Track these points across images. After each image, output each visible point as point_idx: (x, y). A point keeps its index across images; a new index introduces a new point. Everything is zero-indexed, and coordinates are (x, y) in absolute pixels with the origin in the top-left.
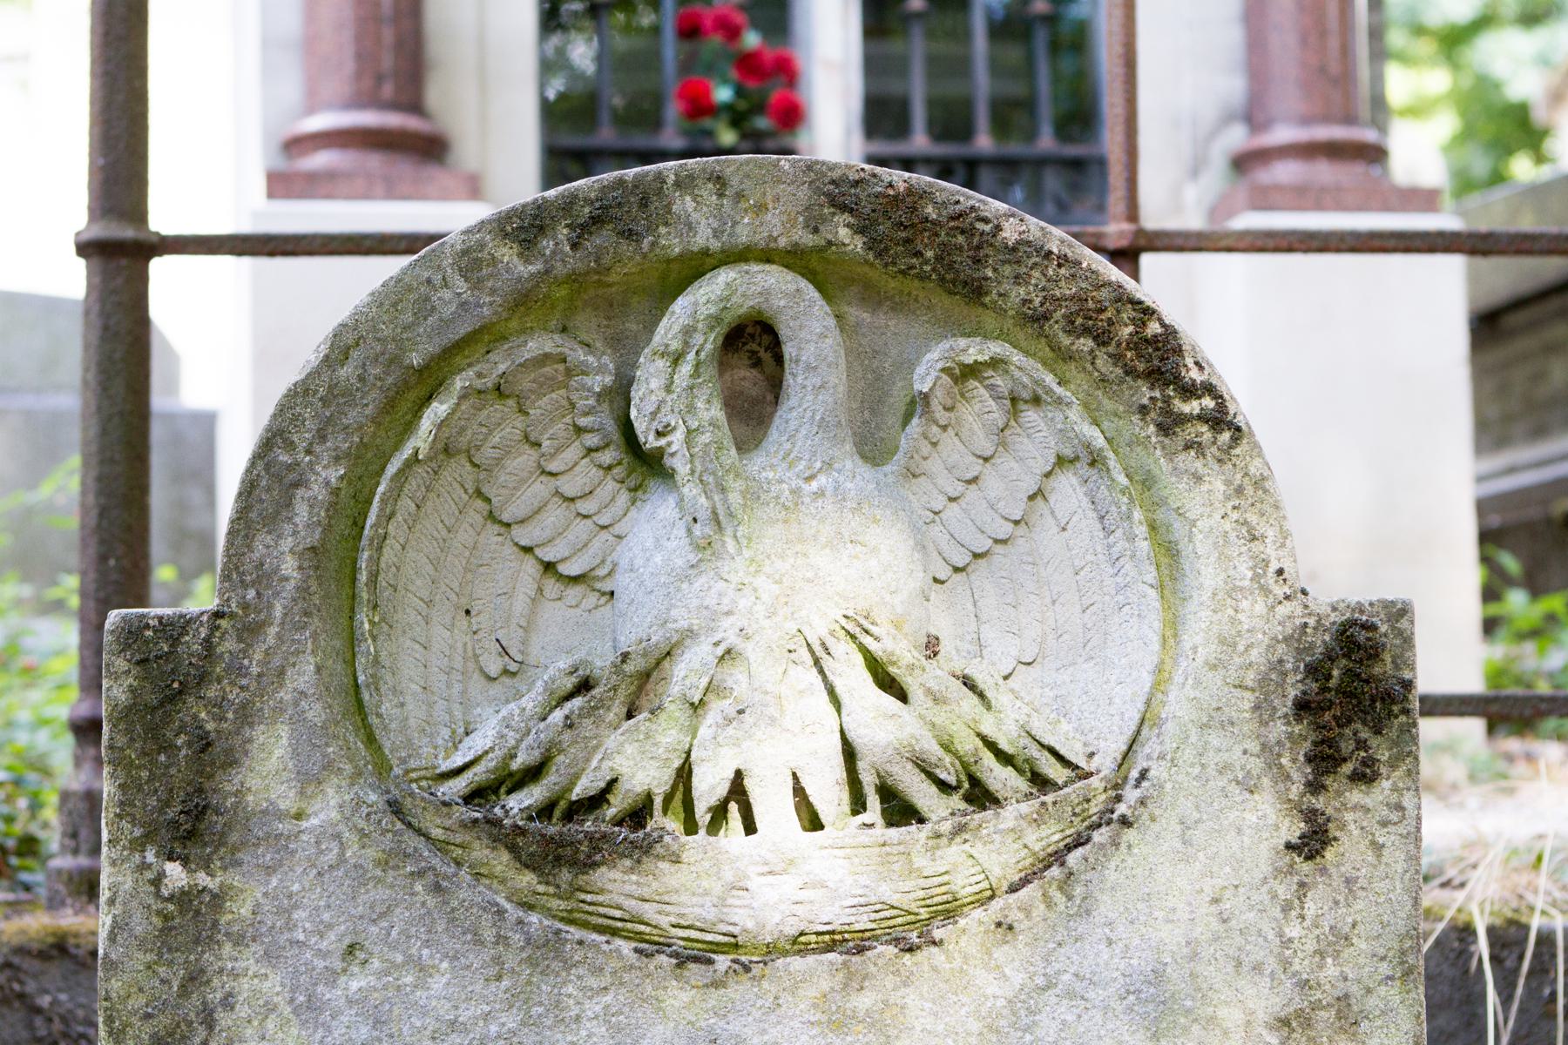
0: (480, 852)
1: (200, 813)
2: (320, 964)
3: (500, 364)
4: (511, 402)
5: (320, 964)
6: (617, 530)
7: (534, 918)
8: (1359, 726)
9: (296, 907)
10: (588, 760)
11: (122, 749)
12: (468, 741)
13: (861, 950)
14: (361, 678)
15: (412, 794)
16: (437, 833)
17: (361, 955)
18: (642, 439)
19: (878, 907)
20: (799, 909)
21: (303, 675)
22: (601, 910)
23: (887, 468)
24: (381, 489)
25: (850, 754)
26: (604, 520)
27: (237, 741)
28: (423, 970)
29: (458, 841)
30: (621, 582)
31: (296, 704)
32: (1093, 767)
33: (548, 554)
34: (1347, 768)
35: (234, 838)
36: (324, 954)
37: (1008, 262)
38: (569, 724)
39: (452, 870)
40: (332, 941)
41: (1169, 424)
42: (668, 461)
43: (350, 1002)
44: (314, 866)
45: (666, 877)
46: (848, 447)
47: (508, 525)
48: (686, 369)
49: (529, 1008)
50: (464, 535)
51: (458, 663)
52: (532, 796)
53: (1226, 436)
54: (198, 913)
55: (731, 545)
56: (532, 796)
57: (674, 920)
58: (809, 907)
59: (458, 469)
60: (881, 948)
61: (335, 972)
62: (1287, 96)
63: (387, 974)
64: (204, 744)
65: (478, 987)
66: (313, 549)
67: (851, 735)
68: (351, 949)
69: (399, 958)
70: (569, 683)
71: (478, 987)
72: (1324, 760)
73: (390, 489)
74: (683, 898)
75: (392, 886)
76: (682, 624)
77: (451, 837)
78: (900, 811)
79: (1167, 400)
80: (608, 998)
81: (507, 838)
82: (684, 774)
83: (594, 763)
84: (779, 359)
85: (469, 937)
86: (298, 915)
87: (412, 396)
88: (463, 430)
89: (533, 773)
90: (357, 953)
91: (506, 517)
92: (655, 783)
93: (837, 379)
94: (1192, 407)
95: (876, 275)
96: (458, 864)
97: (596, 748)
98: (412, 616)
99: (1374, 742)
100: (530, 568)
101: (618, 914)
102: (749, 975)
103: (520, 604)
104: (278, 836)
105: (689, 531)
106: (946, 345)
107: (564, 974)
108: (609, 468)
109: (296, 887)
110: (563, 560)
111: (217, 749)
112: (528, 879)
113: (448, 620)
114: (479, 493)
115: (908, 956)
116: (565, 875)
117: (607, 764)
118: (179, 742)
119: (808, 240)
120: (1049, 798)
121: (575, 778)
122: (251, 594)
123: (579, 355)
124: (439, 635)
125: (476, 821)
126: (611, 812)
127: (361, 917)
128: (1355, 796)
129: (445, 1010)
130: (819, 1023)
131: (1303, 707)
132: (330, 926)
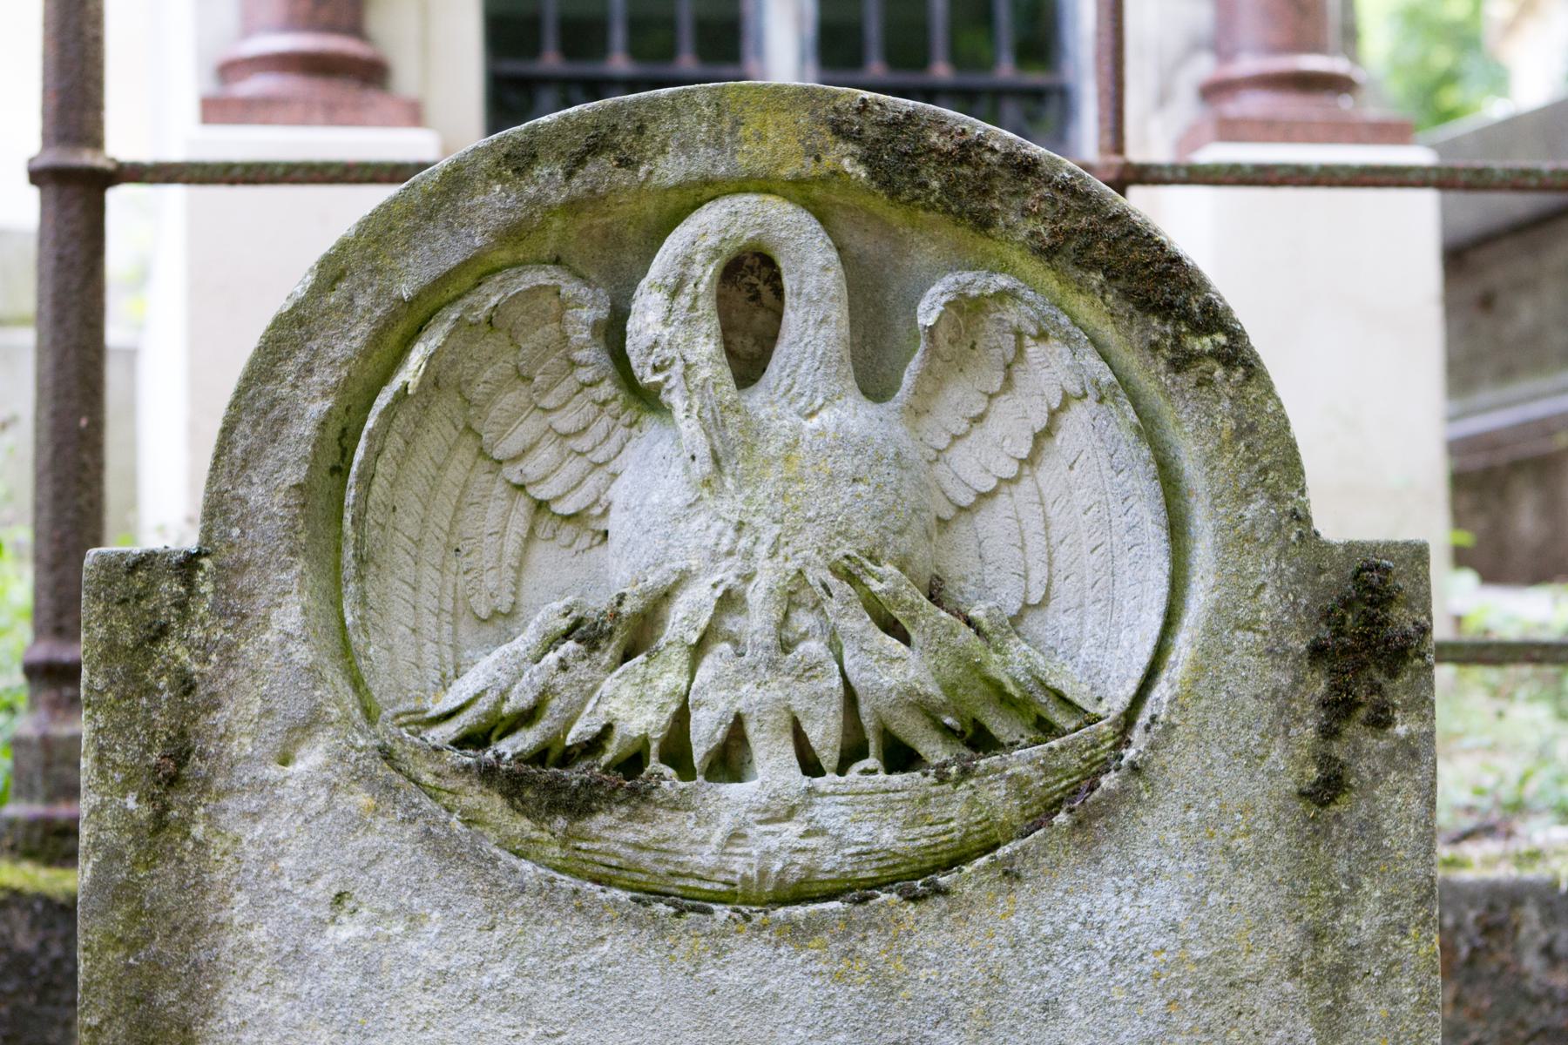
0: (474, 796)
1: (181, 756)
2: (308, 913)
3: (492, 296)
4: (503, 335)
5: (308, 913)
6: (611, 468)
7: (526, 866)
8: (1373, 671)
9: (282, 854)
10: (583, 705)
11: (101, 693)
12: (458, 685)
13: (863, 900)
14: (349, 619)
15: (402, 740)
16: (427, 778)
17: (349, 904)
18: (638, 373)
19: (881, 855)
20: (802, 859)
21: (289, 616)
22: (597, 858)
23: (890, 405)
24: (370, 424)
25: (851, 697)
26: (599, 456)
27: (221, 685)
28: (414, 921)
29: (449, 787)
30: (614, 523)
31: (282, 646)
32: (1101, 710)
33: (542, 493)
34: (1362, 713)
35: (220, 782)
36: (311, 903)
37: (1015, 194)
38: (563, 666)
39: (443, 816)
40: (323, 888)
41: (1181, 362)
42: (664, 397)
43: (339, 952)
44: (300, 812)
45: (665, 826)
46: (851, 383)
47: (500, 462)
48: (684, 300)
49: (524, 958)
50: (455, 473)
51: (448, 605)
52: (526, 740)
53: (1239, 374)
54: (181, 861)
55: (729, 483)
56: (526, 740)
57: (671, 868)
58: (810, 855)
59: (445, 405)
60: (883, 897)
61: (322, 922)
63: (377, 922)
64: (187, 685)
65: (470, 937)
66: (298, 487)
67: (854, 678)
68: (340, 898)
69: (389, 907)
70: (564, 624)
71: (470, 937)
72: (1339, 708)
73: (378, 426)
74: (682, 846)
75: (382, 833)
76: (679, 564)
77: (442, 784)
78: (900, 757)
79: (1177, 338)
80: (606, 948)
82: (682, 717)
83: (589, 707)
84: (779, 292)
85: (461, 885)
86: (286, 863)
87: (401, 328)
88: (454, 363)
89: (527, 717)
90: (346, 902)
91: (497, 454)
92: (652, 728)
93: (839, 313)
94: (1204, 343)
95: (879, 203)
96: (449, 810)
97: (593, 690)
98: (401, 556)
99: (1387, 687)
100: (522, 507)
101: (614, 862)
102: (750, 924)
103: (512, 544)
104: (264, 783)
105: (687, 469)
106: (950, 279)
107: (559, 923)
108: (605, 403)
109: (281, 835)
110: (558, 498)
111: (201, 692)
112: (524, 825)
113: (437, 560)
114: (469, 428)
115: (912, 905)
116: (560, 822)
117: (603, 708)
118: (161, 685)
119: (810, 168)
120: (1055, 743)
121: (569, 723)
122: (236, 532)
123: (570, 288)
124: (429, 576)
125: (467, 767)
126: (606, 758)
127: (350, 865)
128: (1368, 741)
129: (436, 961)
130: (821, 973)
131: (1317, 652)
132: (318, 875)
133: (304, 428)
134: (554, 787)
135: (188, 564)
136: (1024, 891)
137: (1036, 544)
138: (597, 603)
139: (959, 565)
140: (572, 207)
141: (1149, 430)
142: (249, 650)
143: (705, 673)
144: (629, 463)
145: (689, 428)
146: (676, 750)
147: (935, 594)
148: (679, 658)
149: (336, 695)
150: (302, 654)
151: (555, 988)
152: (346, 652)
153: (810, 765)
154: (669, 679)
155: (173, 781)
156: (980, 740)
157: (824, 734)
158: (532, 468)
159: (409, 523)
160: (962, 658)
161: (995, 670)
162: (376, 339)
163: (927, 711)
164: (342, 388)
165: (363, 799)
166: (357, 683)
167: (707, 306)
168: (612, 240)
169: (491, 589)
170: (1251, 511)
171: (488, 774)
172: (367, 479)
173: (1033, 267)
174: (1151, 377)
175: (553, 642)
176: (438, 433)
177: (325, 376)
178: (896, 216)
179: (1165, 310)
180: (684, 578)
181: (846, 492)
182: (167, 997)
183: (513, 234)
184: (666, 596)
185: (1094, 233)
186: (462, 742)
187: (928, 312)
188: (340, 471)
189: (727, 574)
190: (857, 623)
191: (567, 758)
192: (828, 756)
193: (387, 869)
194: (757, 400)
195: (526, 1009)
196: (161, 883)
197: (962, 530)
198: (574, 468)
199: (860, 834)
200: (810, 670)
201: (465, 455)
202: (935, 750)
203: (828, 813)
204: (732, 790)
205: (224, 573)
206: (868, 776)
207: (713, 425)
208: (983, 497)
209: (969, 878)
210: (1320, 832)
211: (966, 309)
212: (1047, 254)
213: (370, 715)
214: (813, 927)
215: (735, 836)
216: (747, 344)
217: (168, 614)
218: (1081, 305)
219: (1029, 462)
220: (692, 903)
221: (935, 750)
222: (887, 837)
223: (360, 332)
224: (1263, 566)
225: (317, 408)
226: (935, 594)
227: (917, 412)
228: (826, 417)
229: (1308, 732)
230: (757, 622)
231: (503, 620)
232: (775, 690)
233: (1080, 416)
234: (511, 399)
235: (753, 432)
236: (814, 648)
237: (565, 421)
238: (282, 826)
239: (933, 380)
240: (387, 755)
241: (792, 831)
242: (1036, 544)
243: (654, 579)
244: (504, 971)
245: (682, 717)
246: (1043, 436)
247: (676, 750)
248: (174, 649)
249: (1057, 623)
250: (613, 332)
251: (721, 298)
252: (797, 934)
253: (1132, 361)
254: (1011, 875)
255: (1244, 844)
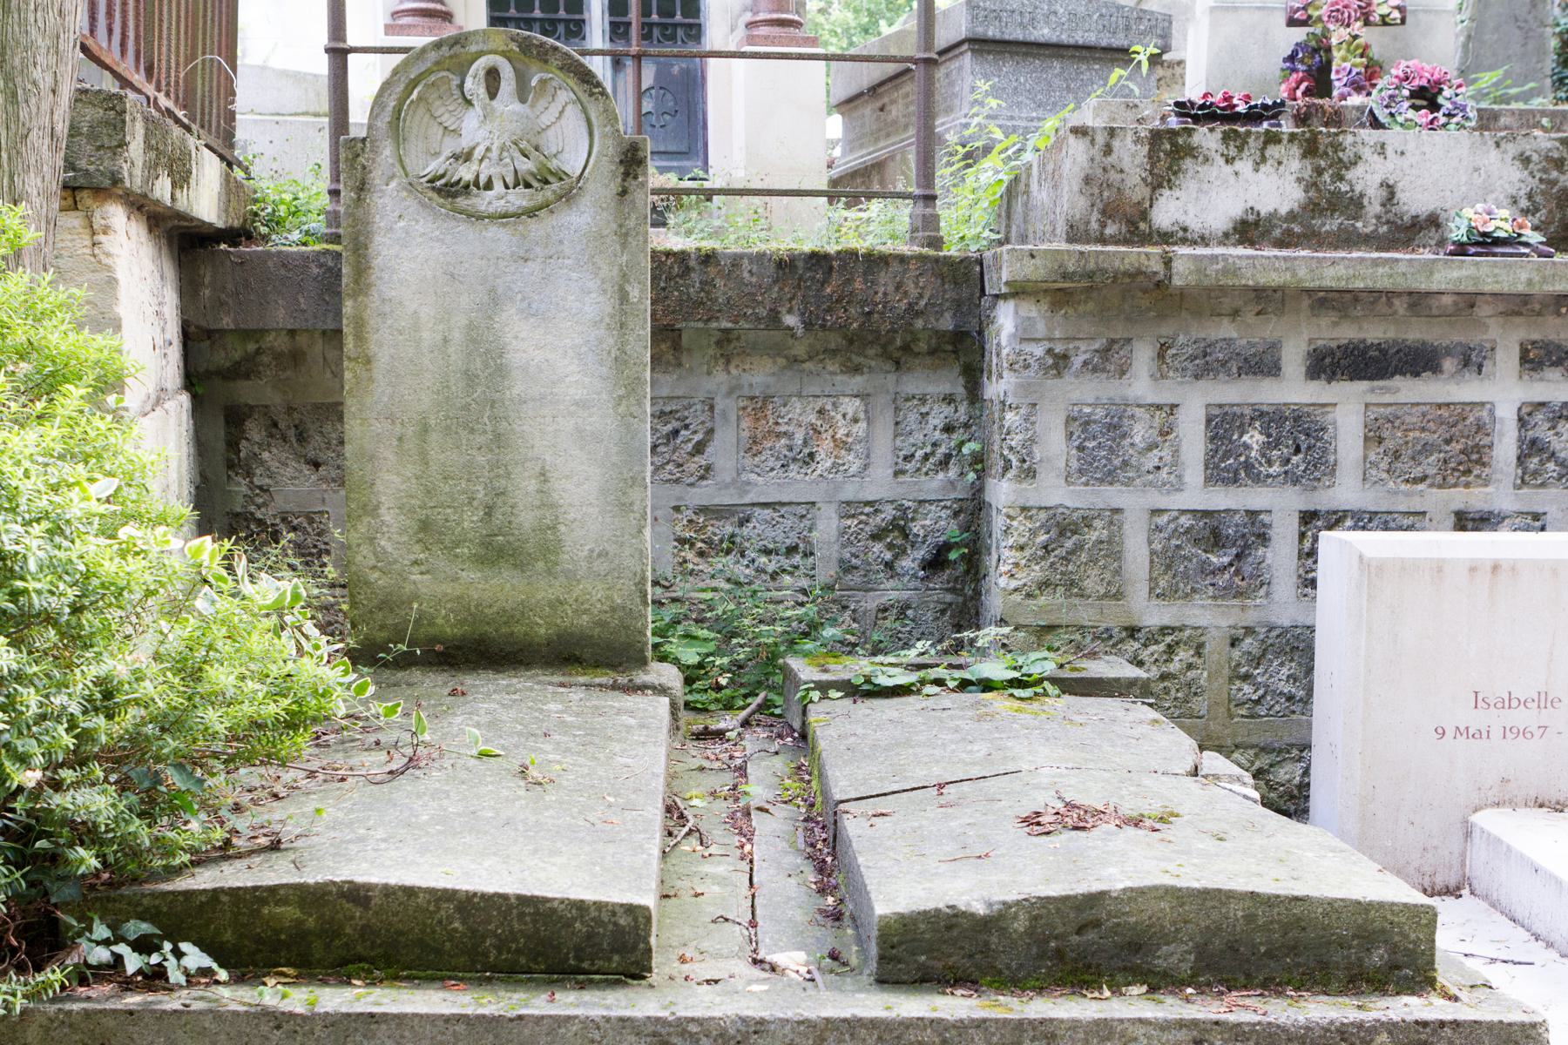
0: (431, 194)
1: (364, 184)
3: (433, 78)
21: (387, 152)
25: (516, 171)
28: (417, 221)
30: (463, 132)
40: (396, 214)
41: (592, 94)
45: (474, 200)
52: (443, 181)
56: (443, 181)
64: (364, 167)
72: (626, 175)
78: (528, 186)
82: (478, 176)
89: (442, 176)
93: (513, 83)
95: (522, 57)
103: (439, 137)
123: (451, 76)
128: (633, 182)
131: (621, 162)
133: (390, 108)
134: (448, 191)
135: (364, 140)
136: (555, 216)
137: (560, 137)
138: (458, 151)
139: (542, 143)
140: (451, 57)
141: (584, 110)
142: (378, 160)
143: (483, 166)
144: (466, 118)
145: (478, 108)
147: (537, 149)
148: (477, 162)
149: (398, 170)
150: (390, 161)
151: (449, 237)
152: (401, 161)
153: (507, 187)
154: (474, 167)
155: (362, 189)
156: (547, 182)
157: (510, 180)
158: (443, 119)
159: (415, 131)
160: (541, 163)
161: (549, 165)
162: (406, 88)
163: (534, 176)
164: (399, 99)
165: (405, 194)
166: (403, 168)
167: (482, 81)
168: (461, 65)
169: (435, 147)
170: (607, 129)
171: (433, 189)
172: (405, 120)
173: (558, 72)
174: (584, 98)
175: (448, 159)
176: (421, 111)
177: (394, 96)
178: (527, 60)
179: (587, 82)
180: (478, 144)
181: (515, 124)
182: (361, 238)
183: (437, 63)
184: (474, 148)
185: (571, 64)
186: (428, 182)
187: (534, 83)
188: (398, 119)
189: (487, 143)
190: (517, 154)
191: (452, 186)
192: (511, 185)
193: (411, 210)
194: (494, 103)
195: (443, 241)
196: (360, 213)
197: (543, 134)
198: (453, 119)
199: (518, 203)
200: (506, 165)
201: (428, 116)
202: (535, 184)
203: (510, 198)
204: (489, 192)
205: (372, 142)
206: (521, 189)
207: (484, 108)
208: (548, 127)
211: (543, 82)
212: (561, 69)
213: (407, 175)
214: (507, 223)
215: (490, 203)
216: (492, 90)
217: (359, 151)
218: (569, 81)
219: (558, 118)
222: (524, 203)
223: (402, 86)
224: (610, 142)
225: (393, 104)
226: (537, 149)
227: (532, 106)
228: (510, 107)
229: (619, 180)
230: (494, 154)
231: (437, 154)
232: (498, 170)
233: (569, 107)
234: (438, 103)
235: (493, 110)
236: (508, 160)
237: (451, 108)
238: (387, 200)
240: (410, 184)
241: (502, 202)
242: (560, 137)
243: (471, 144)
244: (438, 233)
245: (478, 176)
246: (561, 112)
248: (361, 159)
249: (565, 156)
250: (461, 86)
251: (486, 80)
252: (504, 225)
253: (580, 94)
254: (552, 212)
255: (604, 205)
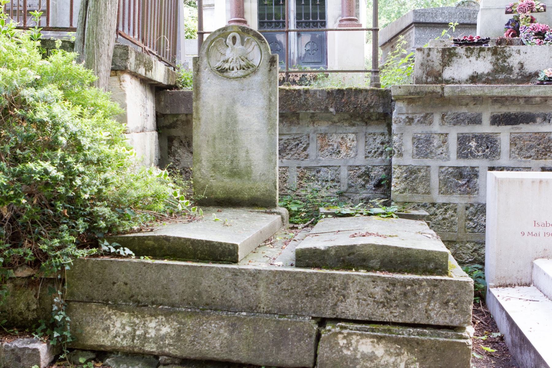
1: (199, 69)
3: (218, 40)
21: (205, 61)
62: (345, 14)
72: (271, 65)
78: (244, 69)
81: (219, 71)
93: (240, 40)
139: (248, 57)
141: (260, 47)
146: (229, 69)
147: (246, 58)
149: (208, 65)
154: (229, 64)
156: (249, 68)
157: (239, 67)
174: (259, 44)
176: (215, 49)
183: (219, 35)
187: (245, 40)
190: (241, 60)
194: (235, 46)
195: (220, 85)
196: (197, 78)
202: (246, 68)
207: (232, 48)
209: (247, 77)
210: (270, 73)
211: (248, 40)
220: (230, 79)
221: (246, 68)
224: (266, 56)
226: (246, 58)
230: (234, 60)
231: (219, 61)
238: (205, 74)
239: (246, 44)
247: (229, 69)
249: (254, 60)
250: (226, 41)
